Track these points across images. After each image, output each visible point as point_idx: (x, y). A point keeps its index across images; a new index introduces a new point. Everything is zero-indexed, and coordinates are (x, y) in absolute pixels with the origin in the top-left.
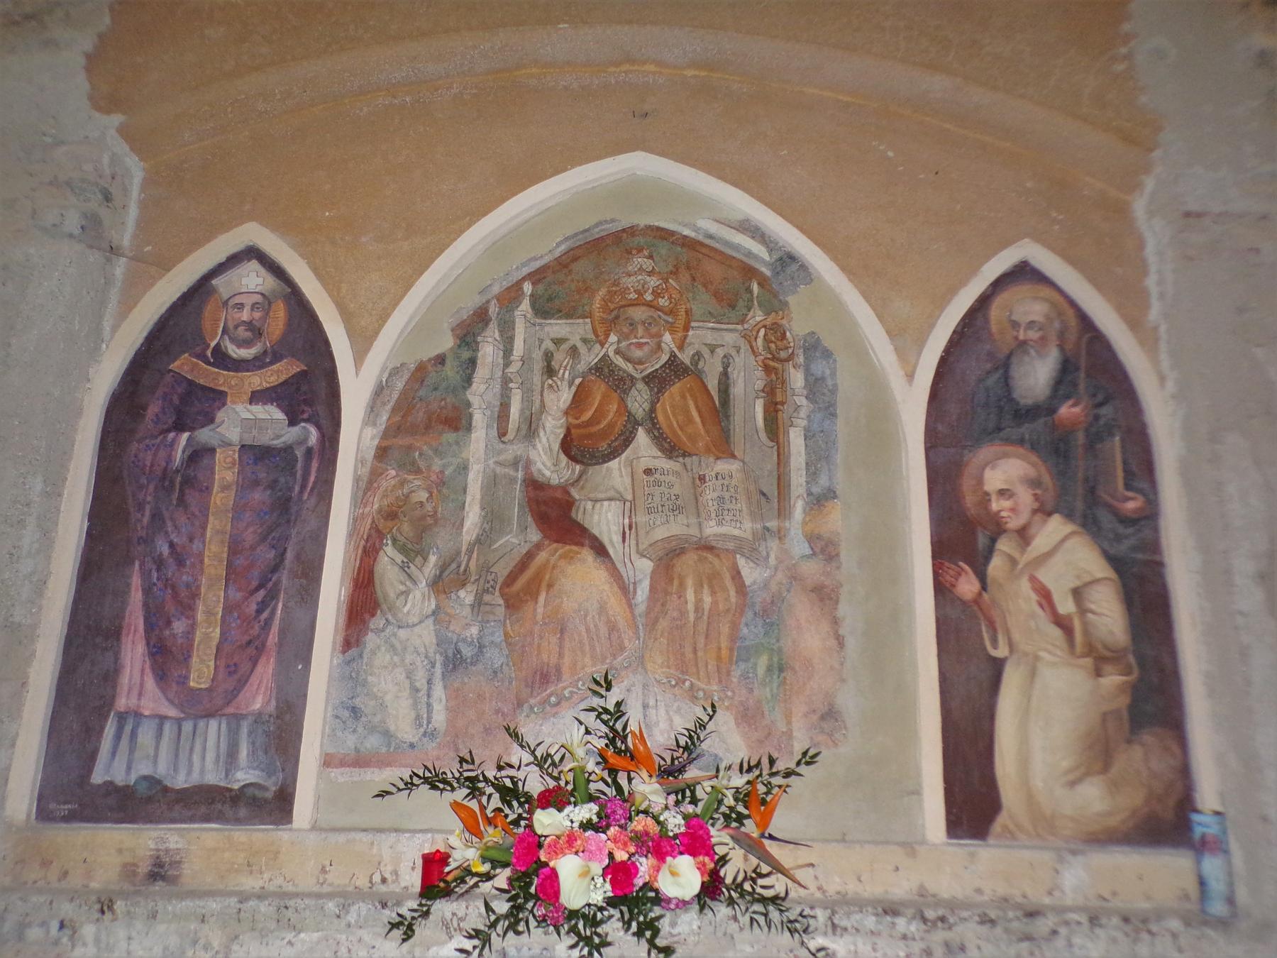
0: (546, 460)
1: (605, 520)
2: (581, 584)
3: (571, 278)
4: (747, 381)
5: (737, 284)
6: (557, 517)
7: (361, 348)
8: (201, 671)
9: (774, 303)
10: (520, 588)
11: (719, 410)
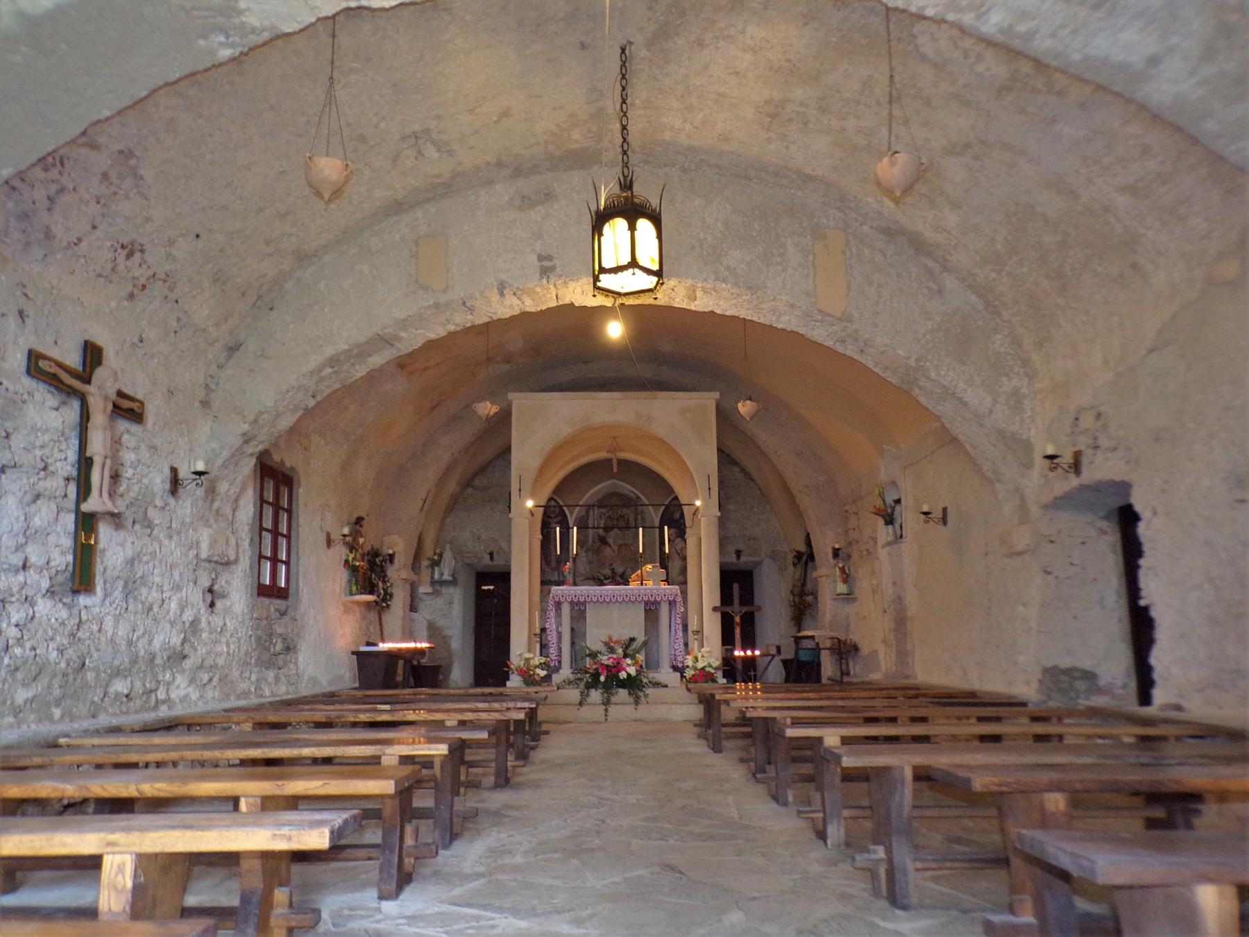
0: (601, 532)
1: (610, 541)
2: (608, 551)
4: (632, 518)
6: (603, 541)
7: (571, 514)
8: (553, 564)
10: (598, 551)
11: (628, 522)
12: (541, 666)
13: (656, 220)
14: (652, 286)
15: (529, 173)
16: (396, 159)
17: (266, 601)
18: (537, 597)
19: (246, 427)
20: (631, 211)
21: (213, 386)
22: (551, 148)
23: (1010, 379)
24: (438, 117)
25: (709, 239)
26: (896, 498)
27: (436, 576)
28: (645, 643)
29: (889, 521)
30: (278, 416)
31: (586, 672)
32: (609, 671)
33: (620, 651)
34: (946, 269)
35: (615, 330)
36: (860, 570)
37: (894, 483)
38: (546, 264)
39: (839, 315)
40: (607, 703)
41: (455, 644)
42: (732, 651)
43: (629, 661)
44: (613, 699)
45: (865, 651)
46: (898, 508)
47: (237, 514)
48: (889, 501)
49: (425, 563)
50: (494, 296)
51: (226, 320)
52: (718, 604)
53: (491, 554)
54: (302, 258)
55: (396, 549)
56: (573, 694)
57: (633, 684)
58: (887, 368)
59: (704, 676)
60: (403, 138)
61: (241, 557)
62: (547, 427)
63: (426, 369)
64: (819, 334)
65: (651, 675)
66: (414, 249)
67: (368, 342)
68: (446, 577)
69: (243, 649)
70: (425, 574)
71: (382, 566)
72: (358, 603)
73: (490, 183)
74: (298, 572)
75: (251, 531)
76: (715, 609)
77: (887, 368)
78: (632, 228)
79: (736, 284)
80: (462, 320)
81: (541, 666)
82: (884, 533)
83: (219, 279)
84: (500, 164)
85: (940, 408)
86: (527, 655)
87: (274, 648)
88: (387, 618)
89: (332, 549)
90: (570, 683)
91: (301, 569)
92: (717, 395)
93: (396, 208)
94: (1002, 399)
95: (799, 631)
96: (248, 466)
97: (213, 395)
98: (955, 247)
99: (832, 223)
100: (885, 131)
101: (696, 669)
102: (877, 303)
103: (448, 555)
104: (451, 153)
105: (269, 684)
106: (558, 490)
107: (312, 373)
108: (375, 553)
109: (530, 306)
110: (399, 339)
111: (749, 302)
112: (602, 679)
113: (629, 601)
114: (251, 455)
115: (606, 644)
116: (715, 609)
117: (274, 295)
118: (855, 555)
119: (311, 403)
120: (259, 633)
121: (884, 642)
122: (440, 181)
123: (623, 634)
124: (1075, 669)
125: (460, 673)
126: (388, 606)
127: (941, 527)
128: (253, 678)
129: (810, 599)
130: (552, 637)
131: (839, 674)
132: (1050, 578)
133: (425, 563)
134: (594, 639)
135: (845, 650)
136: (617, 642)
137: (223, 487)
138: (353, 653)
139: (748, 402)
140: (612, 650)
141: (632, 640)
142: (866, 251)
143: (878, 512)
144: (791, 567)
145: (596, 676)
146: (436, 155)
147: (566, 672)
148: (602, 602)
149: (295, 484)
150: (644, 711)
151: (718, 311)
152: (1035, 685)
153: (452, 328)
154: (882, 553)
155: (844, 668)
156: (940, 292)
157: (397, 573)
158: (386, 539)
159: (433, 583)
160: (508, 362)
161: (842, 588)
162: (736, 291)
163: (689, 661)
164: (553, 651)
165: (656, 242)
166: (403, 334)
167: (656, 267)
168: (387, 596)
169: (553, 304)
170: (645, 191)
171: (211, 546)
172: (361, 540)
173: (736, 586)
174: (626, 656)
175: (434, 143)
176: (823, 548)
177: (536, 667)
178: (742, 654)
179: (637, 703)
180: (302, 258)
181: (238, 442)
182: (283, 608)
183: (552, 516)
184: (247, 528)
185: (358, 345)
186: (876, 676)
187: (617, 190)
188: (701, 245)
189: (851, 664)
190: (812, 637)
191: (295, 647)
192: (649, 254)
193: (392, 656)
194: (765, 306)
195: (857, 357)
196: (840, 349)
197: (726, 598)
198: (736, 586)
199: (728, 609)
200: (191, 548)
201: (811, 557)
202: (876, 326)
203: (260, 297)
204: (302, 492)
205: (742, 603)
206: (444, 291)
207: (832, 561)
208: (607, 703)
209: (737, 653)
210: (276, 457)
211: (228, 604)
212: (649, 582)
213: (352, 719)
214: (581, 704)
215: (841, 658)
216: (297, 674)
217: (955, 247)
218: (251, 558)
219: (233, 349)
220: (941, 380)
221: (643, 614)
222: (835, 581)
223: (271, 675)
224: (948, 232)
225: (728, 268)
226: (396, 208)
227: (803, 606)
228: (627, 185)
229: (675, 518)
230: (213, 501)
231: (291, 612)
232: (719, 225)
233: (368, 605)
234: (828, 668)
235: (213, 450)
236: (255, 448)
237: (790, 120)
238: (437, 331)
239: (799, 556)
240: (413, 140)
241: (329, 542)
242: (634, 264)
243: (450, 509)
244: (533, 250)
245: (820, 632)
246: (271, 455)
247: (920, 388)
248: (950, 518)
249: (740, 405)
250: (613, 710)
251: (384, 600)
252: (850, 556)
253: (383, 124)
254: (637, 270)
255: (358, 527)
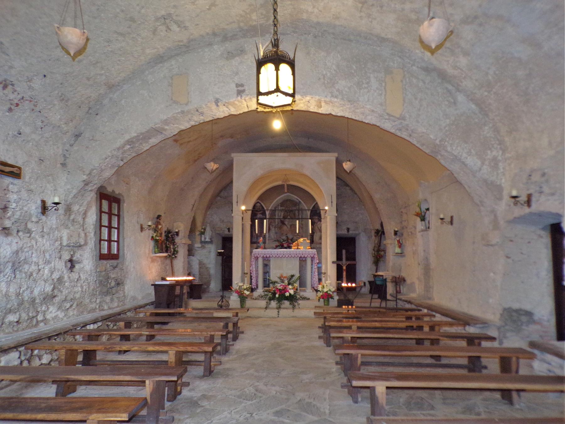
1: (286, 223)
2: (285, 228)
3: (283, 203)
5: (295, 204)
6: (283, 223)
9: (298, 205)
10: (280, 228)
12: (247, 289)
13: (292, 64)
14: (290, 102)
15: (228, 38)
16: (154, 32)
17: (105, 262)
18: (248, 252)
19: (85, 177)
20: (277, 58)
21: (67, 156)
22: (242, 24)
23: (492, 152)
24: (175, 6)
25: (329, 74)
26: (427, 208)
27: (203, 239)
28: (300, 278)
29: (423, 219)
30: (102, 170)
31: (270, 292)
32: (280, 292)
33: (286, 282)
34: (458, 90)
35: (277, 125)
36: (407, 242)
37: (426, 200)
38: (240, 88)
39: (398, 116)
40: (279, 308)
41: (212, 271)
42: (341, 284)
43: (290, 287)
44: (282, 306)
45: (408, 281)
46: (428, 212)
47: (86, 220)
48: (423, 209)
49: (197, 233)
50: (214, 107)
51: (72, 121)
52: (335, 259)
53: (229, 229)
54: (111, 87)
55: (180, 229)
56: (263, 303)
57: (292, 299)
58: (423, 145)
59: (327, 297)
60: (157, 19)
61: (89, 242)
62: (251, 172)
63: (189, 142)
64: (387, 126)
65: (302, 294)
66: (171, 81)
67: (147, 132)
68: (207, 240)
69: (92, 288)
70: (198, 238)
71: (173, 238)
72: (160, 257)
73: (210, 44)
74: (124, 246)
75: (95, 228)
76: (333, 262)
77: (423, 145)
78: (277, 69)
79: (342, 99)
80: (197, 119)
81: (247, 289)
82: (420, 225)
83: (63, 99)
84: (214, 34)
85: (452, 166)
86: (241, 284)
87: (109, 285)
88: (175, 262)
89: (144, 232)
90: (262, 297)
91: (126, 245)
92: (336, 155)
93: (160, 59)
94: (487, 163)
95: (376, 272)
96: (91, 196)
97: (67, 161)
98: (465, 78)
99: (396, 65)
100: (426, 9)
101: (323, 291)
102: (419, 110)
103: (208, 229)
104: (186, 28)
105: (107, 303)
106: (261, 198)
107: (118, 149)
108: (168, 232)
109: (233, 111)
110: (165, 130)
111: (350, 108)
112: (277, 296)
113: (290, 257)
114: (91, 191)
115: (280, 278)
116: (333, 262)
117: (98, 107)
118: (405, 235)
119: (122, 163)
120: (101, 278)
121: (418, 278)
122: (182, 44)
123: (287, 273)
124: (521, 310)
125: (215, 285)
126: (176, 257)
127: (450, 226)
128: (98, 301)
129: (382, 253)
130: (254, 275)
131: (395, 292)
132: (510, 261)
133: (197, 233)
134: (274, 275)
135: (399, 281)
136: (285, 277)
137: (75, 208)
138: (152, 285)
139: (348, 163)
140: (283, 282)
141: (292, 276)
142: (414, 81)
143: (417, 215)
144: (373, 237)
145: (274, 294)
146: (178, 29)
147: (260, 291)
148: (278, 257)
149: (121, 202)
150: (297, 312)
151: (333, 113)
152: (498, 316)
153: (193, 123)
154: (419, 235)
155: (398, 289)
156: (455, 103)
157: (181, 241)
158: (175, 224)
159: (201, 242)
160: (232, 138)
161: (398, 250)
162: (342, 102)
163: (320, 288)
164: (254, 281)
165: (292, 76)
166: (166, 127)
167: (291, 92)
168: (175, 252)
169: (246, 110)
170: (286, 47)
171: (69, 239)
172: (160, 227)
173: (344, 252)
174: (289, 284)
175: (176, 22)
176: (389, 229)
177: (245, 289)
178: (346, 285)
179: (294, 307)
180: (111, 87)
181: (82, 184)
182: (115, 264)
183: (257, 212)
184: (92, 227)
185: (142, 134)
186: (413, 295)
187: (270, 47)
188: (324, 79)
189: (401, 287)
190: (382, 276)
191: (123, 283)
192: (287, 84)
193: (172, 287)
194: (358, 111)
195: (408, 138)
196: (399, 134)
197: (339, 257)
198: (344, 252)
199: (340, 263)
200: (57, 241)
201: (383, 233)
202: (418, 122)
203: (90, 108)
204: (125, 206)
205: (347, 259)
206: (187, 104)
207: (393, 236)
208: (279, 308)
209: (344, 285)
210: (110, 189)
211: (82, 266)
212: (302, 247)
213: (119, 349)
214: (266, 308)
215: (396, 284)
216: (124, 296)
217: (465, 78)
218: (95, 242)
219: (77, 136)
220: (453, 152)
221: (298, 263)
222: (395, 246)
223: (108, 299)
224: (461, 69)
225: (338, 90)
226: (160, 59)
227: (379, 257)
228: (276, 44)
229: (316, 214)
230: (70, 215)
231: (120, 266)
232: (334, 66)
233: (166, 257)
234: (390, 289)
235: (68, 189)
236: (94, 186)
237: (373, 5)
238: (185, 125)
239: (377, 232)
240: (163, 20)
241: (142, 229)
242: (277, 90)
243: (209, 207)
244: (233, 81)
245: (386, 273)
246: (106, 188)
247: (442, 156)
248: (455, 221)
249: (344, 164)
250: (282, 312)
251: (174, 254)
252: (402, 234)
253: (143, 11)
254: (279, 94)
255: (158, 220)
